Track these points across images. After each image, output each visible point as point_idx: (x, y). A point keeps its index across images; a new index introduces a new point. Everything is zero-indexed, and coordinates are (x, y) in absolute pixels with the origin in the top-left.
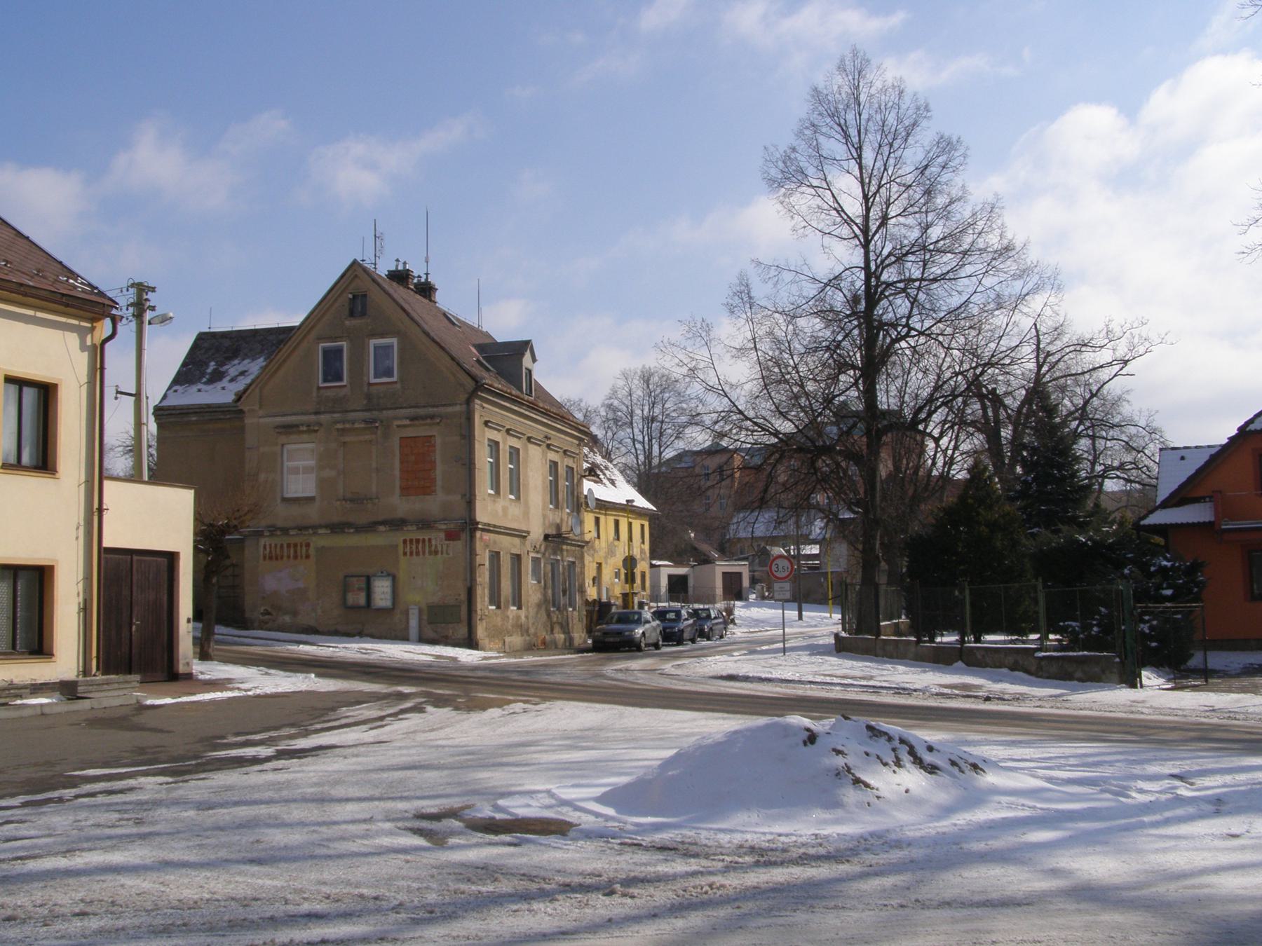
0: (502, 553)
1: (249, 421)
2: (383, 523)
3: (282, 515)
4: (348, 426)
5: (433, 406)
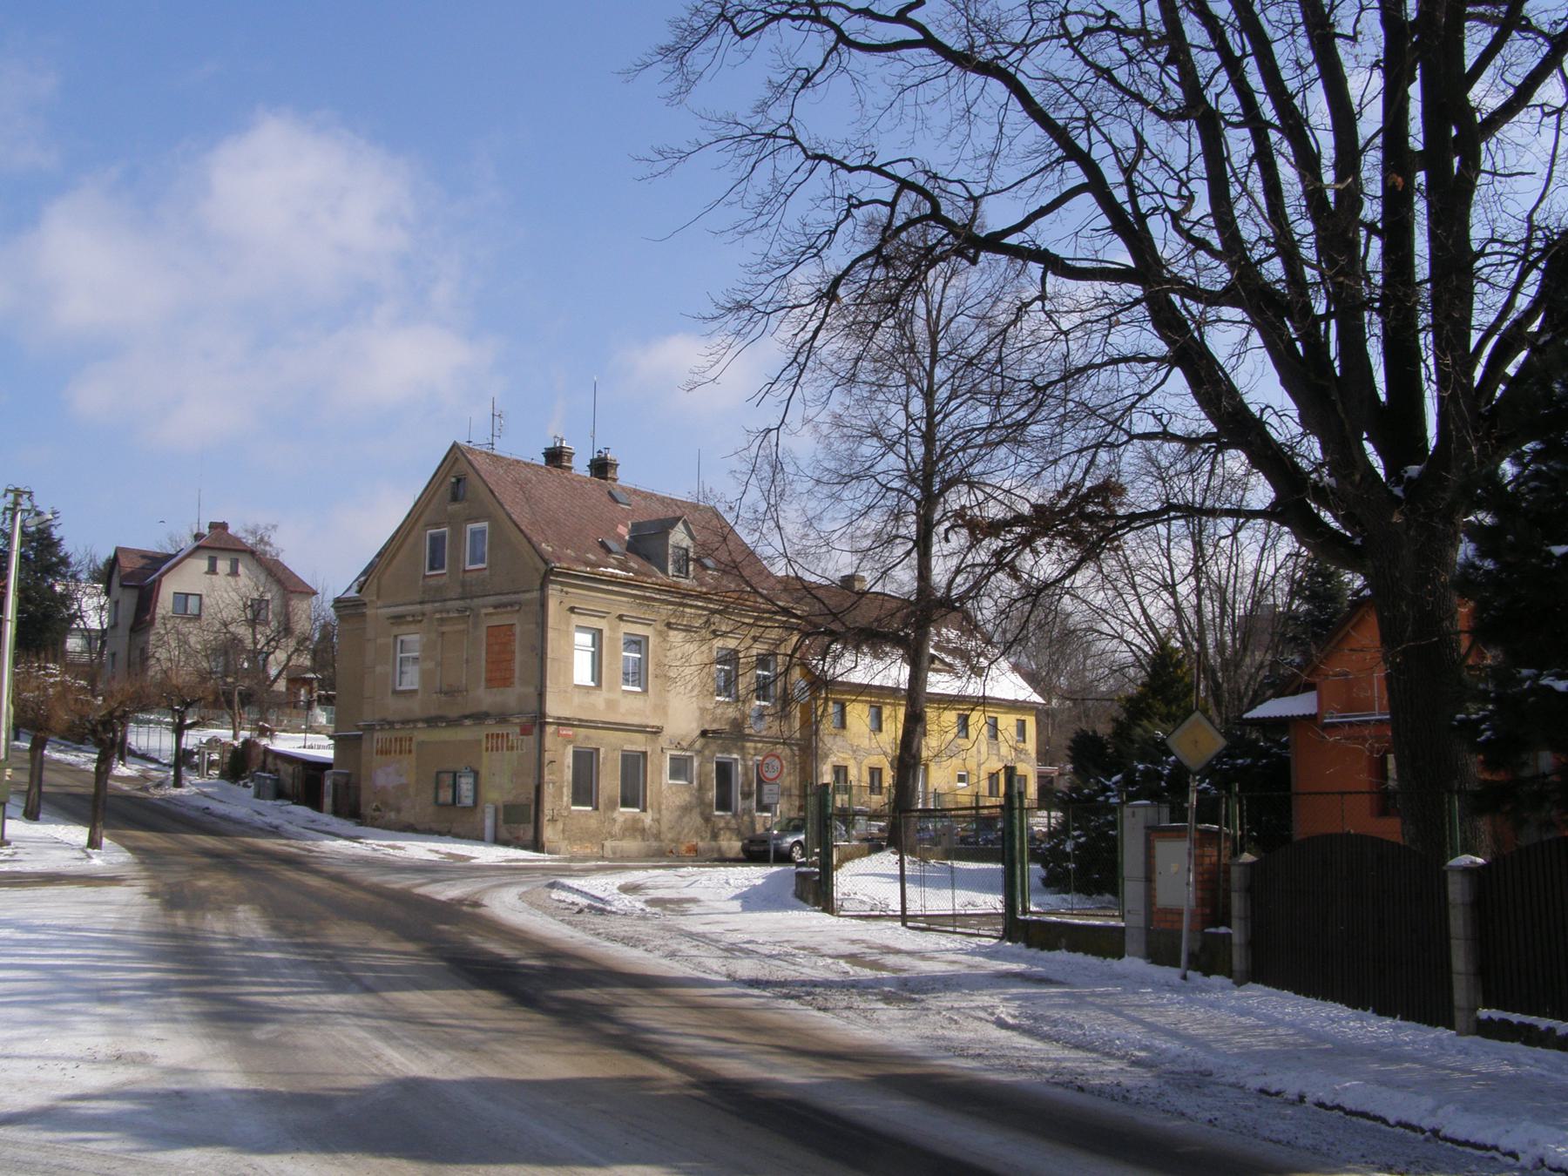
0: (602, 751)
1: (369, 611)
2: (466, 717)
3: (394, 708)
4: (445, 615)
5: (515, 593)
